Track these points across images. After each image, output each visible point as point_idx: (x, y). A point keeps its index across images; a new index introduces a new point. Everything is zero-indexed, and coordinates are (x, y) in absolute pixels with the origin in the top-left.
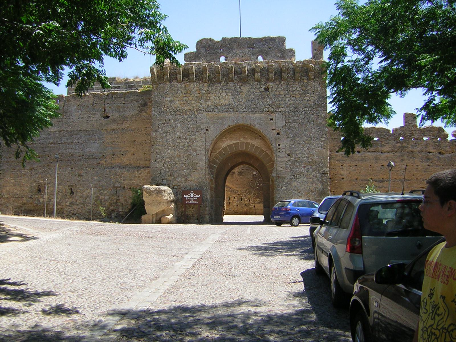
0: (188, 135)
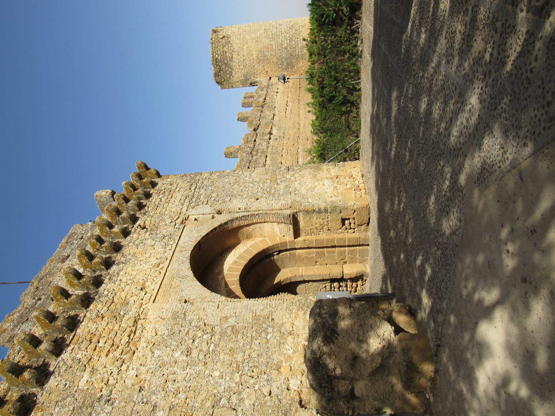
0: (188, 333)
